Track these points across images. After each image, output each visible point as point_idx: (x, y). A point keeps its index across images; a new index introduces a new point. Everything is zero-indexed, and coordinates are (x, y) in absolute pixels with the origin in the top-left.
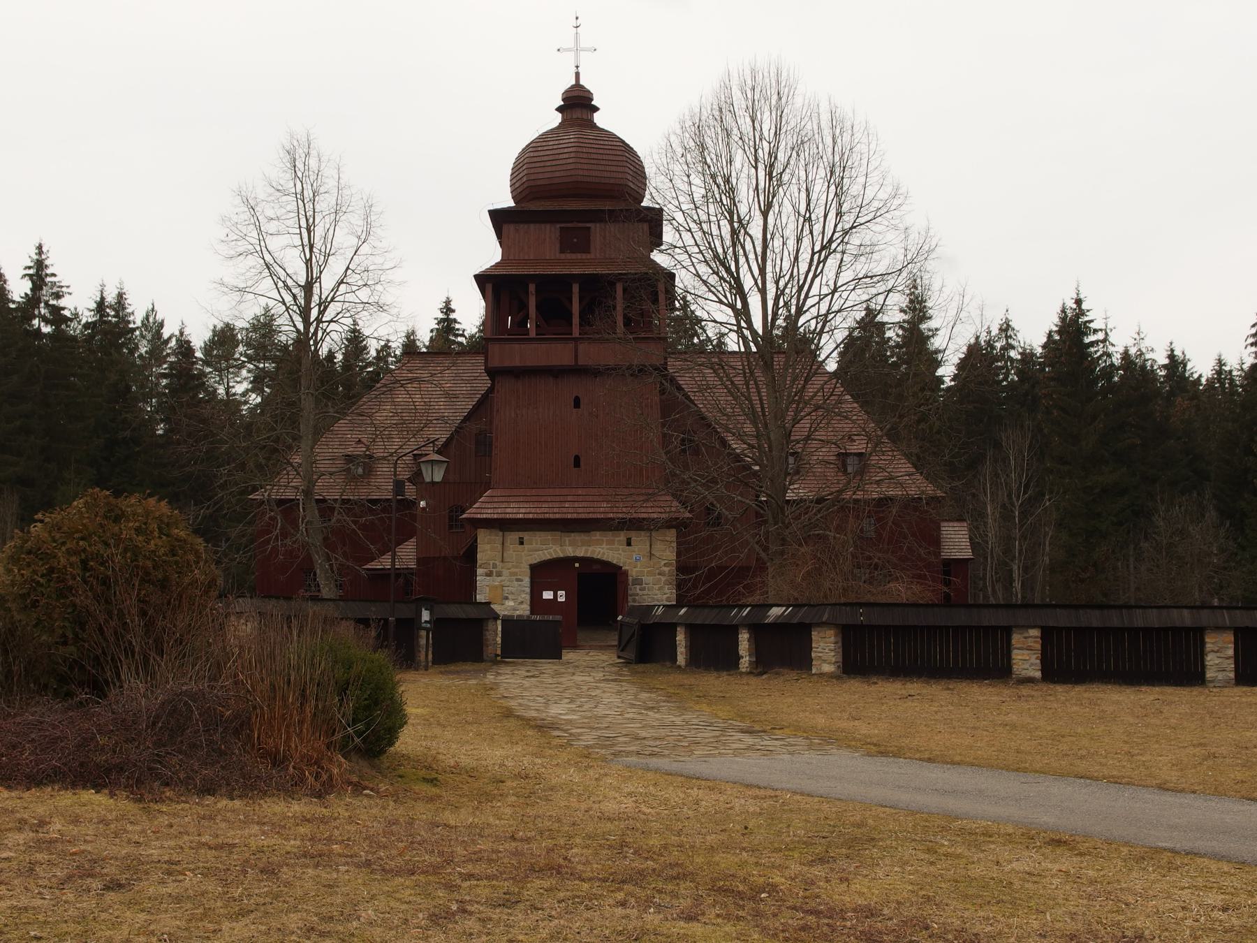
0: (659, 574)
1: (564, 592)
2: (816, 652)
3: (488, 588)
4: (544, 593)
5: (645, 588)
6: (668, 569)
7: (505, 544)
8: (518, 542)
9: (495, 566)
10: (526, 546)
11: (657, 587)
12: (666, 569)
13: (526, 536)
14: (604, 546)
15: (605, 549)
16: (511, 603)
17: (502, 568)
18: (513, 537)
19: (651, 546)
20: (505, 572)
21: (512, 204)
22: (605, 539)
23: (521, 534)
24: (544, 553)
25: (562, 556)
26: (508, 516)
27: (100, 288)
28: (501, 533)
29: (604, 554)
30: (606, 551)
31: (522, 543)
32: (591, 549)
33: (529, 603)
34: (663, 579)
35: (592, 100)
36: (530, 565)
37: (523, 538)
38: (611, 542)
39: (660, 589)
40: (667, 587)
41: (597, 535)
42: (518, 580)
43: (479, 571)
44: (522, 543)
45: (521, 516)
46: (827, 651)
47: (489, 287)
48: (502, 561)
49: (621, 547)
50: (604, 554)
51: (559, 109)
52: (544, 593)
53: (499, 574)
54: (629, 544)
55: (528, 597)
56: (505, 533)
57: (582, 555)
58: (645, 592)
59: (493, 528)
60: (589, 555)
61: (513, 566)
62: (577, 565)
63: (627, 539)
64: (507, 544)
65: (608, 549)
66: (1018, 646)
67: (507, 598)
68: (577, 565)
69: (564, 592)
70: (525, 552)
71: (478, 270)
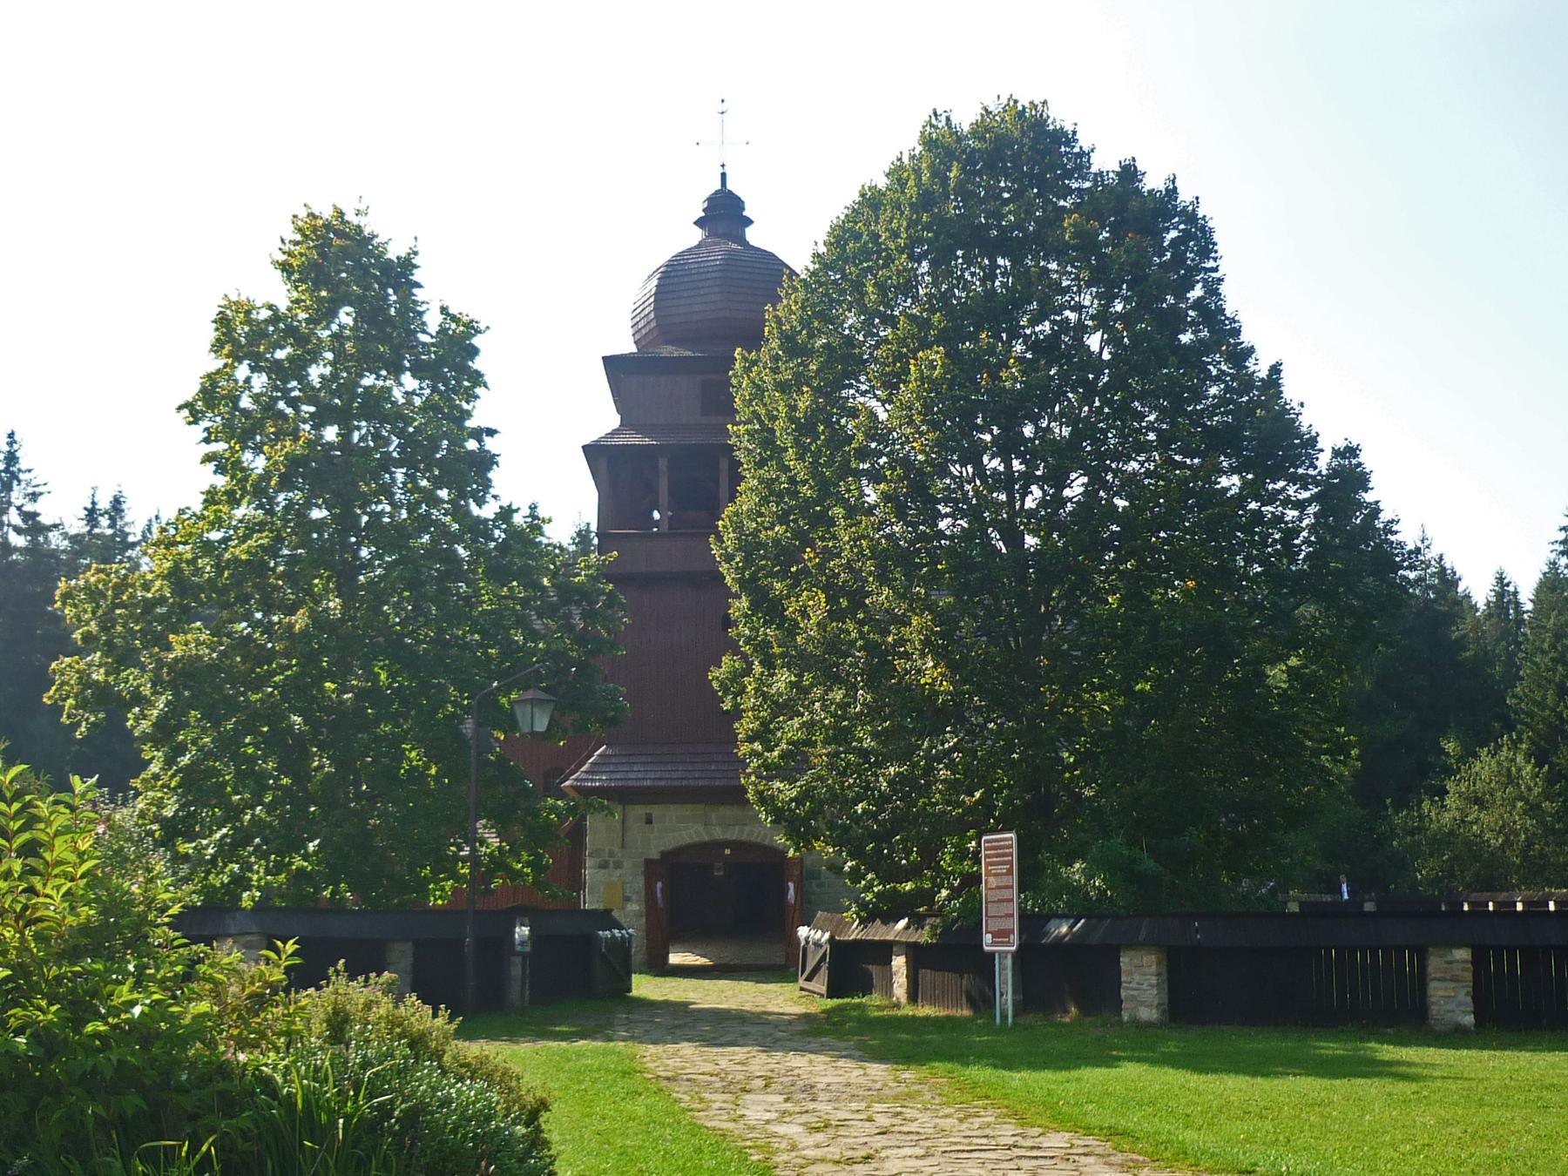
2: (1128, 989)
8: (644, 820)
9: (611, 854)
13: (656, 811)
18: (639, 811)
21: (634, 349)
23: (648, 809)
26: (630, 783)
27: (92, 492)
31: (649, 821)
32: (747, 828)
35: (744, 209)
37: (651, 814)
45: (649, 783)
46: (1145, 987)
47: (603, 464)
48: (623, 846)
51: (699, 223)
53: (618, 865)
56: (630, 807)
57: (734, 838)
60: (744, 837)
66: (1438, 975)
67: (627, 899)
68: (727, 852)
71: (588, 439)
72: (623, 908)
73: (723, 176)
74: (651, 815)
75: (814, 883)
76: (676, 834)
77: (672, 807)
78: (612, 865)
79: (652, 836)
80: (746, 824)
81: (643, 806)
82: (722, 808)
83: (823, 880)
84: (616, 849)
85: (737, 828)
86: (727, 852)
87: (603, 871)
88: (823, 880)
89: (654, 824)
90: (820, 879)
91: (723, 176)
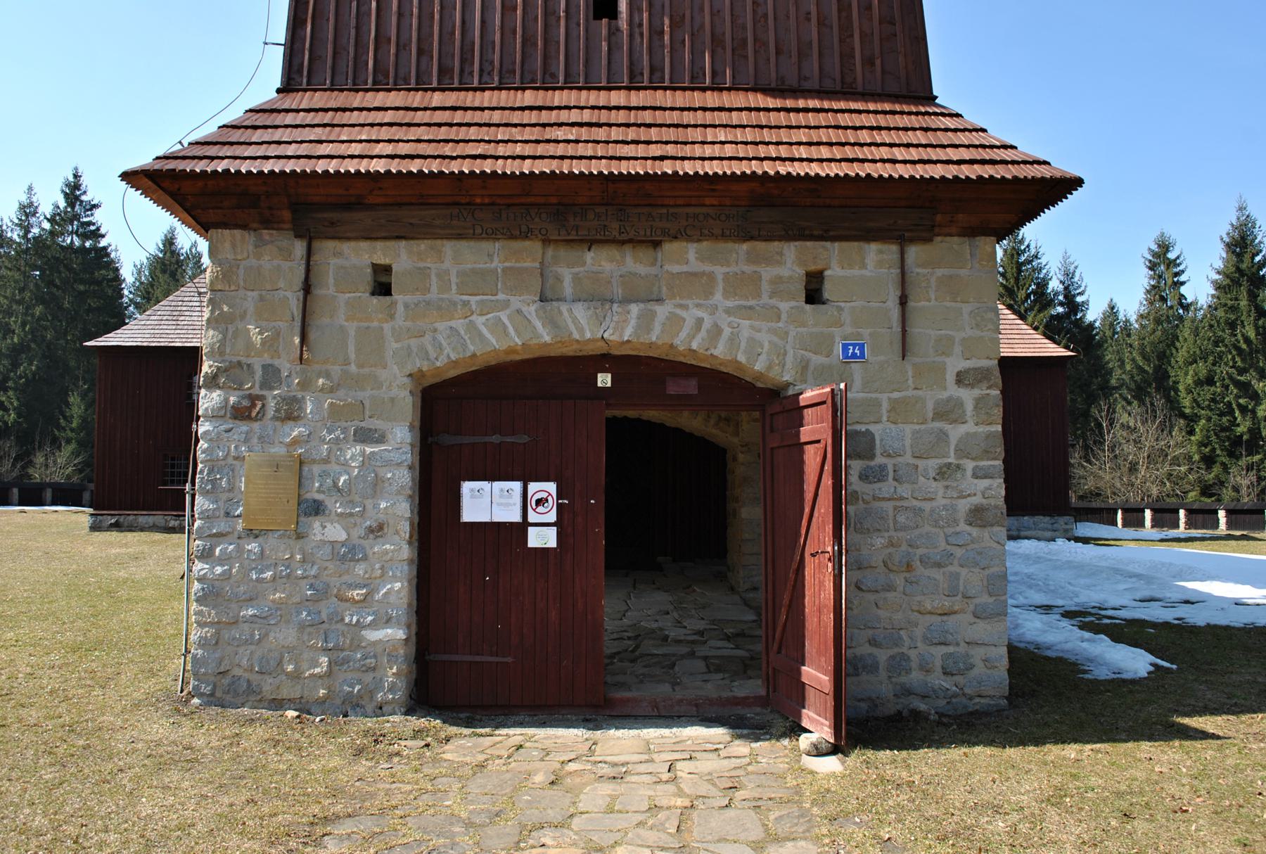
0: (939, 415)
1: (551, 487)
4: (467, 487)
5: (883, 468)
6: (977, 392)
7: (318, 292)
9: (271, 376)
10: (399, 297)
11: (932, 464)
12: (968, 396)
16: (336, 532)
17: (305, 385)
19: (903, 301)
22: (719, 271)
23: (380, 252)
24: (472, 327)
28: (299, 248)
29: (716, 332)
30: (724, 321)
31: (383, 288)
32: (662, 311)
33: (405, 528)
36: (415, 376)
37: (387, 269)
38: (740, 285)
39: (944, 473)
40: (969, 465)
42: (364, 436)
43: (208, 400)
44: (383, 288)
45: (379, 166)
49: (784, 306)
50: (716, 332)
52: (467, 487)
53: (290, 413)
54: (814, 295)
58: (887, 488)
63: (810, 275)
64: (327, 288)
65: (728, 311)
67: (317, 509)
68: (604, 380)
69: (551, 487)
72: (300, 536)
74: (387, 269)
75: (857, 466)
76: (459, 324)
77: (449, 247)
79: (387, 327)
80: (659, 300)
81: (364, 245)
82: (589, 256)
83: (879, 460)
84: (285, 365)
85: (635, 309)
87: (244, 427)
88: (879, 460)
89: (398, 297)
90: (872, 457)
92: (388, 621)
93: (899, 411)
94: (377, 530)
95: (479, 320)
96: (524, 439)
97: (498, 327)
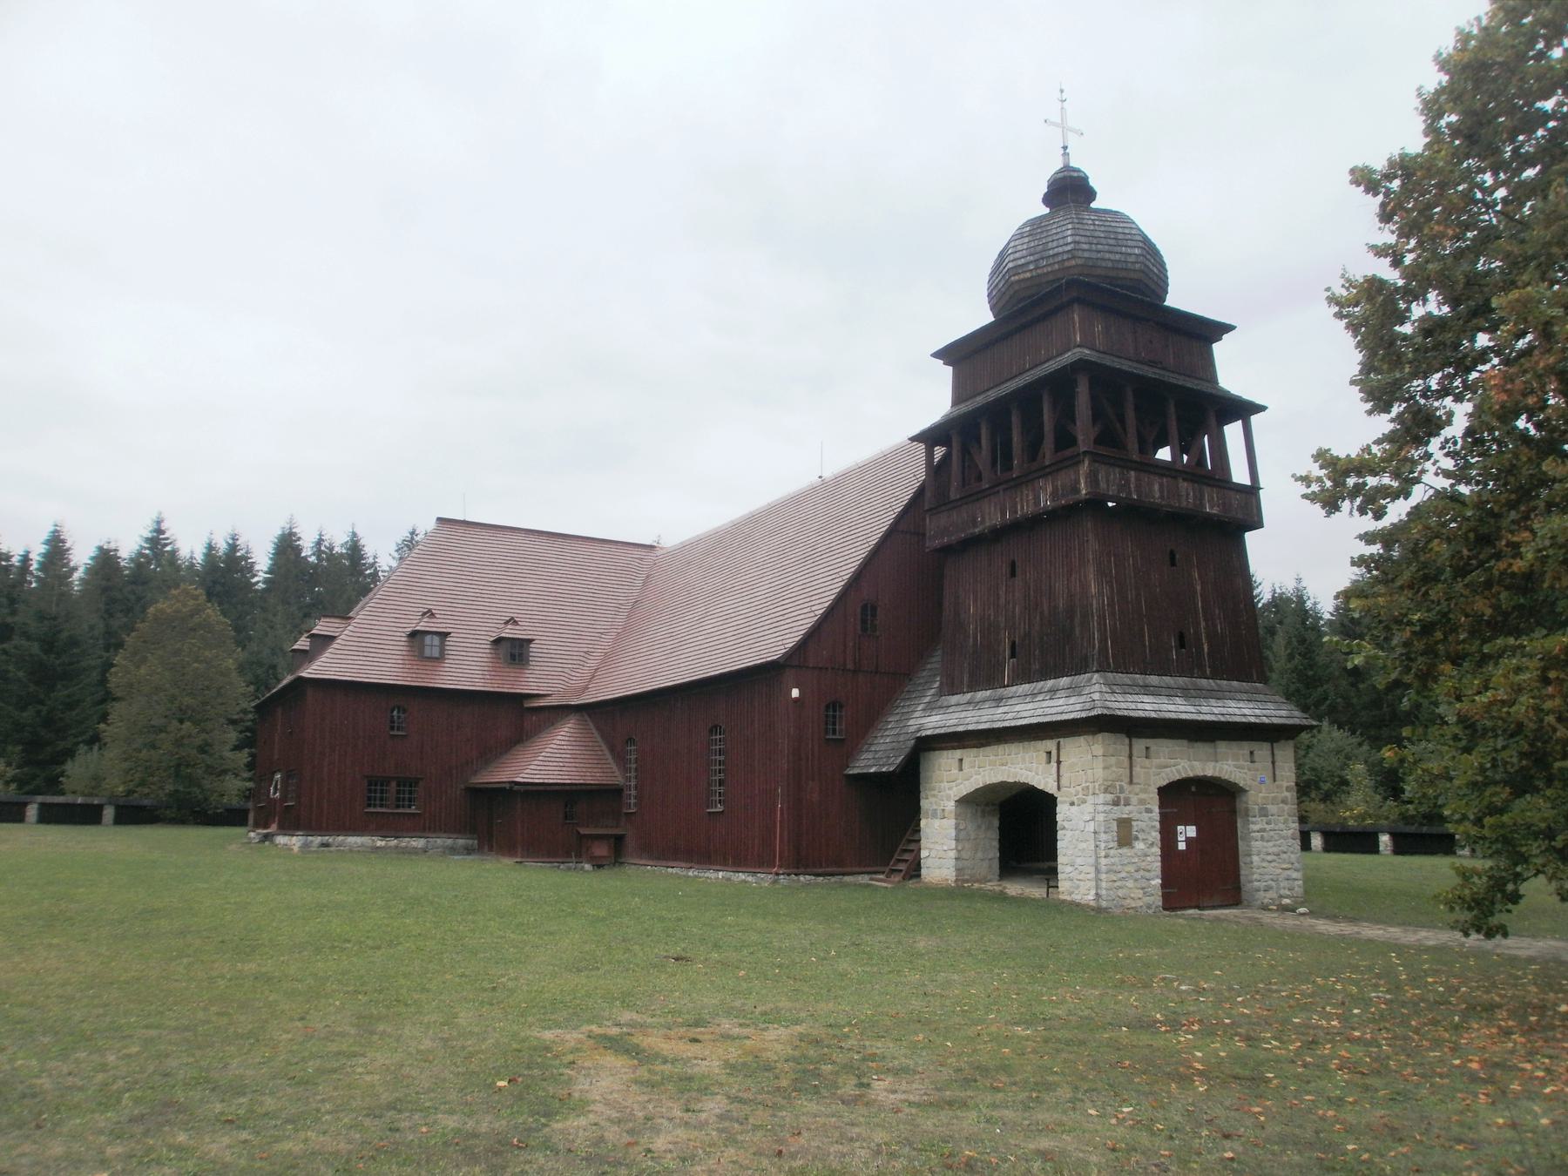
3: (1115, 823)
4: (1194, 828)
9: (1122, 790)
14: (1230, 762)
15: (1227, 764)
17: (1130, 792)
18: (1140, 745)
20: (1134, 800)
24: (1172, 771)
25: (1191, 775)
34: (1286, 807)
38: (1236, 758)
41: (1222, 747)
48: (1131, 782)
52: (1194, 828)
53: (1127, 804)
55: (1158, 836)
56: (1134, 740)
59: (1101, 730)
61: (1142, 791)
62: (1193, 789)
67: (1137, 838)
70: (1154, 769)
73: (1066, 155)
78: (1122, 802)
86: (1193, 789)
91: (1066, 155)
92: (1157, 877)
93: (1274, 801)
94: (1152, 844)
95: (1173, 768)
96: (1175, 810)
97: (1178, 771)
